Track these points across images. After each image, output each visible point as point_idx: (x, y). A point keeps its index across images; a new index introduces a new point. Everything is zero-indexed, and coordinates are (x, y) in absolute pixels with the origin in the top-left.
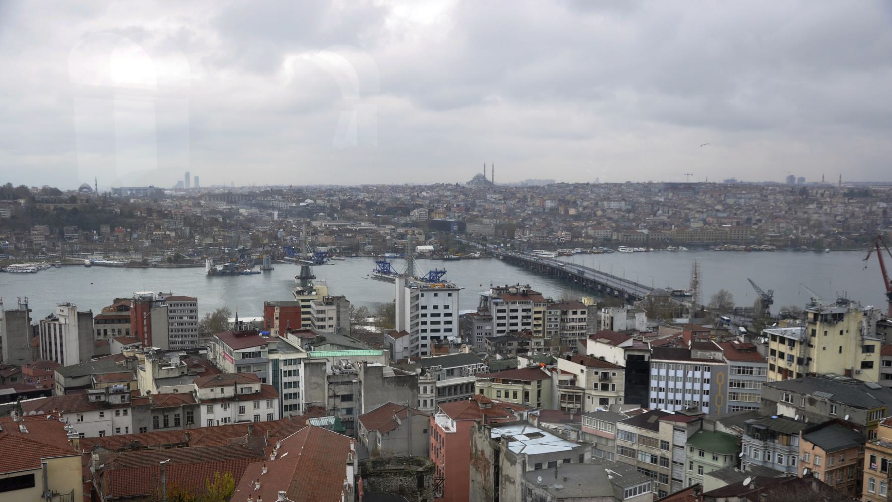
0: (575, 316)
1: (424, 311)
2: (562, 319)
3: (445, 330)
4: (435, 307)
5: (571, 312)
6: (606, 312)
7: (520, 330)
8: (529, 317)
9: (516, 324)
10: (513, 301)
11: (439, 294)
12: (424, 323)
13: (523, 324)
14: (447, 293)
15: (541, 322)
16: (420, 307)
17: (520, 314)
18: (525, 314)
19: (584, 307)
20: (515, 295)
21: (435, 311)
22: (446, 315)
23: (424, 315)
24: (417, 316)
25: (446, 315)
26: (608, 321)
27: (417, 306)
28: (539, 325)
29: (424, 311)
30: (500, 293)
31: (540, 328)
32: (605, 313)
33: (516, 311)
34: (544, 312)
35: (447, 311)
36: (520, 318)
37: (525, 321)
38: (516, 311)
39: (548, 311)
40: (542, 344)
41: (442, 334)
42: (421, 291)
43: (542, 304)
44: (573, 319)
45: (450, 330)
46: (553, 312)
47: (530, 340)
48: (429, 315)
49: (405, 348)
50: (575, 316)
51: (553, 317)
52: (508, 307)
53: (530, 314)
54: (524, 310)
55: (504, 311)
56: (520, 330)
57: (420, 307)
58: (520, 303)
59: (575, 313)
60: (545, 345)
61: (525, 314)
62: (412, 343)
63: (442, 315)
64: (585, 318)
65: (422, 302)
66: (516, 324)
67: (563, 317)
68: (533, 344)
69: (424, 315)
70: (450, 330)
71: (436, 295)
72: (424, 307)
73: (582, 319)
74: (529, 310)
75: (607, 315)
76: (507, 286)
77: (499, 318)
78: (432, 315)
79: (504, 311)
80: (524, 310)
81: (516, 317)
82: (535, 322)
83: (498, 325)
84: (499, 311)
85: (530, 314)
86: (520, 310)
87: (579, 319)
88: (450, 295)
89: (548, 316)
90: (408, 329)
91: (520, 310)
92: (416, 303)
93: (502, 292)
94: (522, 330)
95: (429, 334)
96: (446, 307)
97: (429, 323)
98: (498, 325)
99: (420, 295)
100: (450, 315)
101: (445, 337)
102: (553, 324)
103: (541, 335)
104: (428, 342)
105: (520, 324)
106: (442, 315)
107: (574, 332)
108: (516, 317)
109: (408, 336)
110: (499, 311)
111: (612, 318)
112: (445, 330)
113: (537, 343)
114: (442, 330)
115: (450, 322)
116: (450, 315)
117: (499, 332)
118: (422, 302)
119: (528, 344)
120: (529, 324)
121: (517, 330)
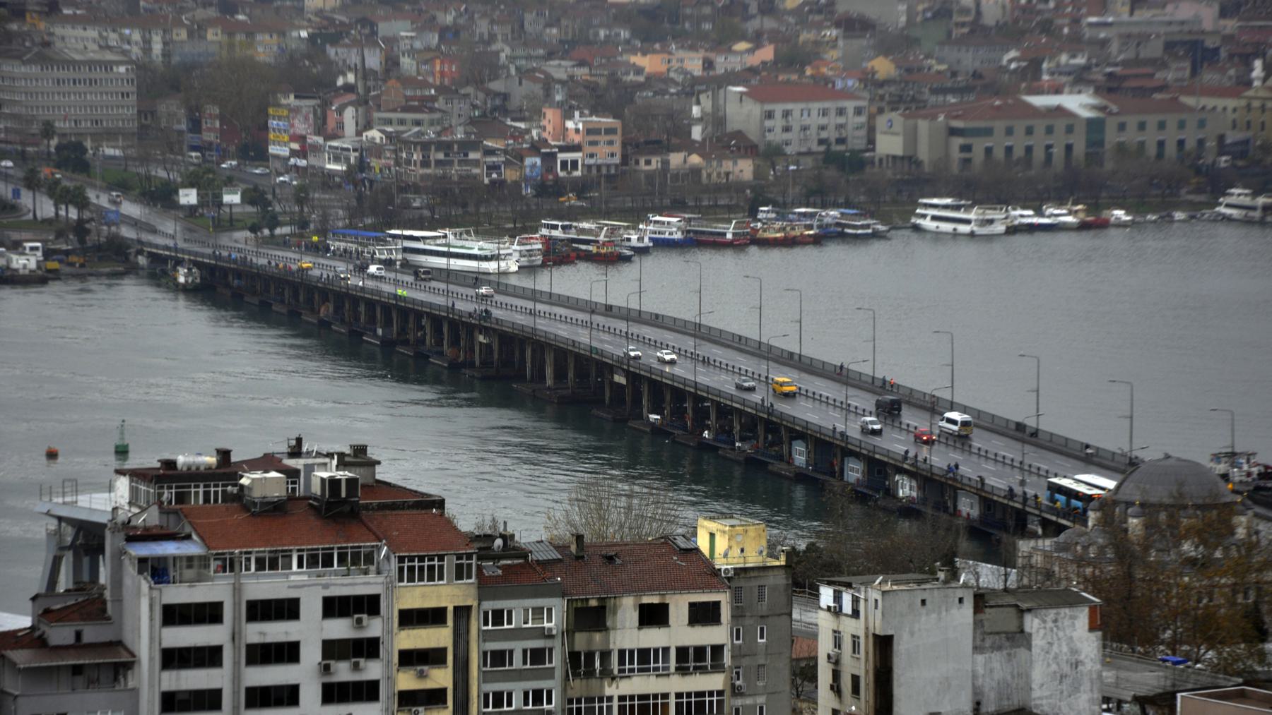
10: (265, 550)
18: (340, 629)
20: (275, 509)
30: (181, 498)
33: (287, 609)
34: (462, 613)
38: (287, 609)
39: (489, 605)
43: (449, 564)
44: (644, 654)
46: (519, 611)
51: (518, 647)
52: (237, 590)
53: (374, 628)
54: (334, 607)
55: (209, 613)
58: (313, 562)
61: (340, 629)
67: (581, 641)
74: (370, 605)
76: (224, 455)
79: (209, 613)
80: (334, 607)
84: (174, 615)
86: (311, 607)
89: (485, 637)
91: (311, 607)
93: (197, 493)
110: (174, 615)
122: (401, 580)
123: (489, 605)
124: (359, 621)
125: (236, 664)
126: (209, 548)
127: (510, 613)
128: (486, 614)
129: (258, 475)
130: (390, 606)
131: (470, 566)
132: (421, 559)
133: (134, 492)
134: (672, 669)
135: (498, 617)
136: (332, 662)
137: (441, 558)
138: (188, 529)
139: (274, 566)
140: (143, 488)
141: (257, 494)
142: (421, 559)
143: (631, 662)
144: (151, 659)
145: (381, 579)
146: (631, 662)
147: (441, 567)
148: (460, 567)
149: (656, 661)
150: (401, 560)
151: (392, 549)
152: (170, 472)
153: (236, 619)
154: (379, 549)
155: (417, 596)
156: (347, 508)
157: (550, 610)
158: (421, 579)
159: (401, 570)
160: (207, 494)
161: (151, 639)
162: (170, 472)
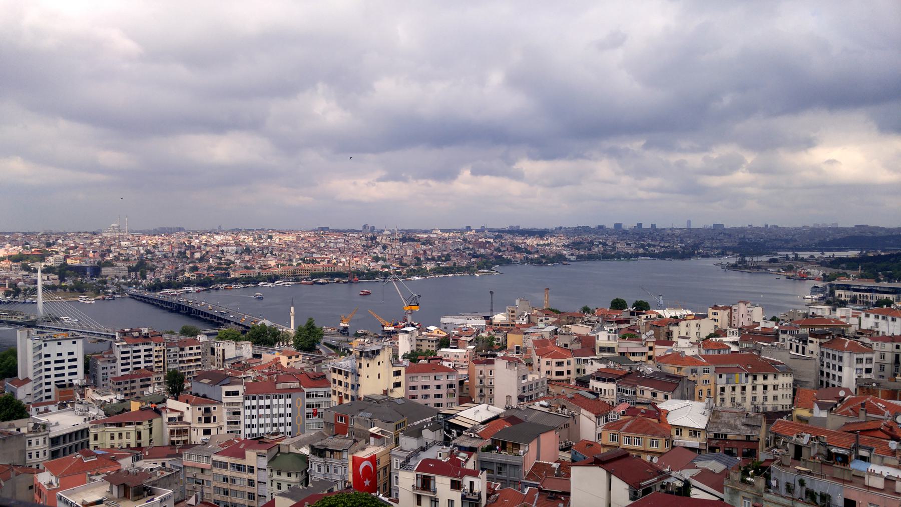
0: (191, 352)
1: (47, 359)
2: (180, 355)
3: (70, 374)
4: (60, 355)
5: (187, 348)
6: (218, 345)
7: (143, 368)
8: (151, 356)
9: (139, 363)
10: (136, 343)
11: (62, 342)
12: (49, 370)
13: (146, 362)
14: (71, 341)
15: (161, 359)
16: (43, 356)
17: (142, 354)
18: (147, 353)
19: (199, 343)
21: (60, 358)
22: (70, 360)
23: (48, 363)
24: (40, 364)
25: (70, 360)
26: (221, 353)
27: (40, 355)
28: (161, 361)
29: (47, 359)
30: (125, 335)
31: (161, 364)
32: (217, 346)
33: (139, 351)
35: (71, 357)
36: (143, 357)
37: (147, 359)
38: (139, 351)
39: (168, 349)
40: (162, 378)
41: (66, 378)
42: (43, 341)
43: (162, 344)
44: (190, 354)
45: (75, 373)
46: (172, 350)
47: (151, 376)
48: (53, 362)
49: (27, 395)
50: (191, 352)
53: (151, 353)
54: (146, 350)
55: (128, 352)
56: (143, 368)
57: (43, 356)
58: (142, 344)
59: (191, 349)
60: (164, 380)
61: (147, 353)
62: (35, 390)
63: (66, 361)
64: (200, 353)
65: (45, 351)
66: (139, 363)
67: (181, 353)
68: (154, 379)
69: (48, 363)
70: (75, 373)
71: (59, 344)
72: (48, 356)
73: (198, 353)
74: (151, 350)
75: (219, 348)
77: (123, 359)
78: (56, 362)
79: (128, 352)
80: (146, 350)
81: (139, 357)
82: (156, 360)
83: (123, 364)
84: (123, 353)
85: (151, 353)
86: (142, 351)
87: (195, 353)
88: (74, 343)
89: (167, 353)
90: (31, 376)
91: (142, 351)
92: (39, 352)
94: (145, 367)
95: (53, 380)
96: (71, 353)
97: (53, 369)
98: (123, 364)
99: (43, 346)
100: (75, 360)
101: (71, 380)
102: (172, 360)
103: (162, 370)
104: (52, 386)
105: (143, 362)
106: (66, 361)
107: (191, 364)
108: (139, 357)
109: (31, 383)
110: (123, 353)
111: (223, 350)
112: (70, 374)
113: (157, 378)
114: (67, 375)
115: (75, 367)
116: (75, 360)
117: (123, 370)
118: (45, 351)
119: (149, 380)
120: (151, 361)
121: (140, 368)
123: (168, 349)
135: (169, 350)
139: (137, 345)
155: (158, 348)
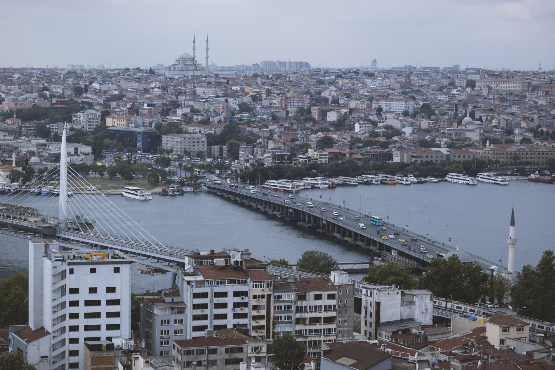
10: (219, 280)
18: (238, 300)
20: (221, 269)
30: (201, 263)
33: (224, 295)
34: (269, 296)
38: (224, 295)
39: (276, 294)
46: (285, 296)
51: (283, 305)
52: (212, 290)
53: (246, 300)
54: (236, 294)
55: (205, 295)
58: (231, 282)
61: (238, 300)
67: (299, 304)
74: (245, 294)
76: (212, 251)
79: (205, 295)
80: (236, 294)
84: (196, 296)
86: (231, 294)
89: (275, 302)
91: (231, 294)
93: (205, 262)
110: (196, 296)
122: (253, 287)
123: (276, 294)
124: (243, 298)
125: (211, 308)
126: (205, 279)
127: (281, 296)
128: (275, 296)
129: (218, 259)
130: (250, 294)
131: (271, 284)
132: (259, 282)
133: (190, 261)
134: (323, 311)
136: (236, 308)
137: (264, 282)
138: (200, 273)
139: (221, 283)
140: (191, 260)
141: (217, 265)
142: (259, 282)
143: (312, 309)
144: (190, 307)
145: (248, 287)
146: (312, 309)
147: (264, 284)
148: (268, 284)
149: (319, 309)
150: (253, 282)
151: (251, 280)
152: (199, 256)
153: (211, 297)
154: (248, 279)
155: (258, 291)
156: (240, 268)
157: (292, 295)
158: (258, 287)
159: (253, 285)
160: (207, 262)
161: (190, 302)
162: (199, 256)
